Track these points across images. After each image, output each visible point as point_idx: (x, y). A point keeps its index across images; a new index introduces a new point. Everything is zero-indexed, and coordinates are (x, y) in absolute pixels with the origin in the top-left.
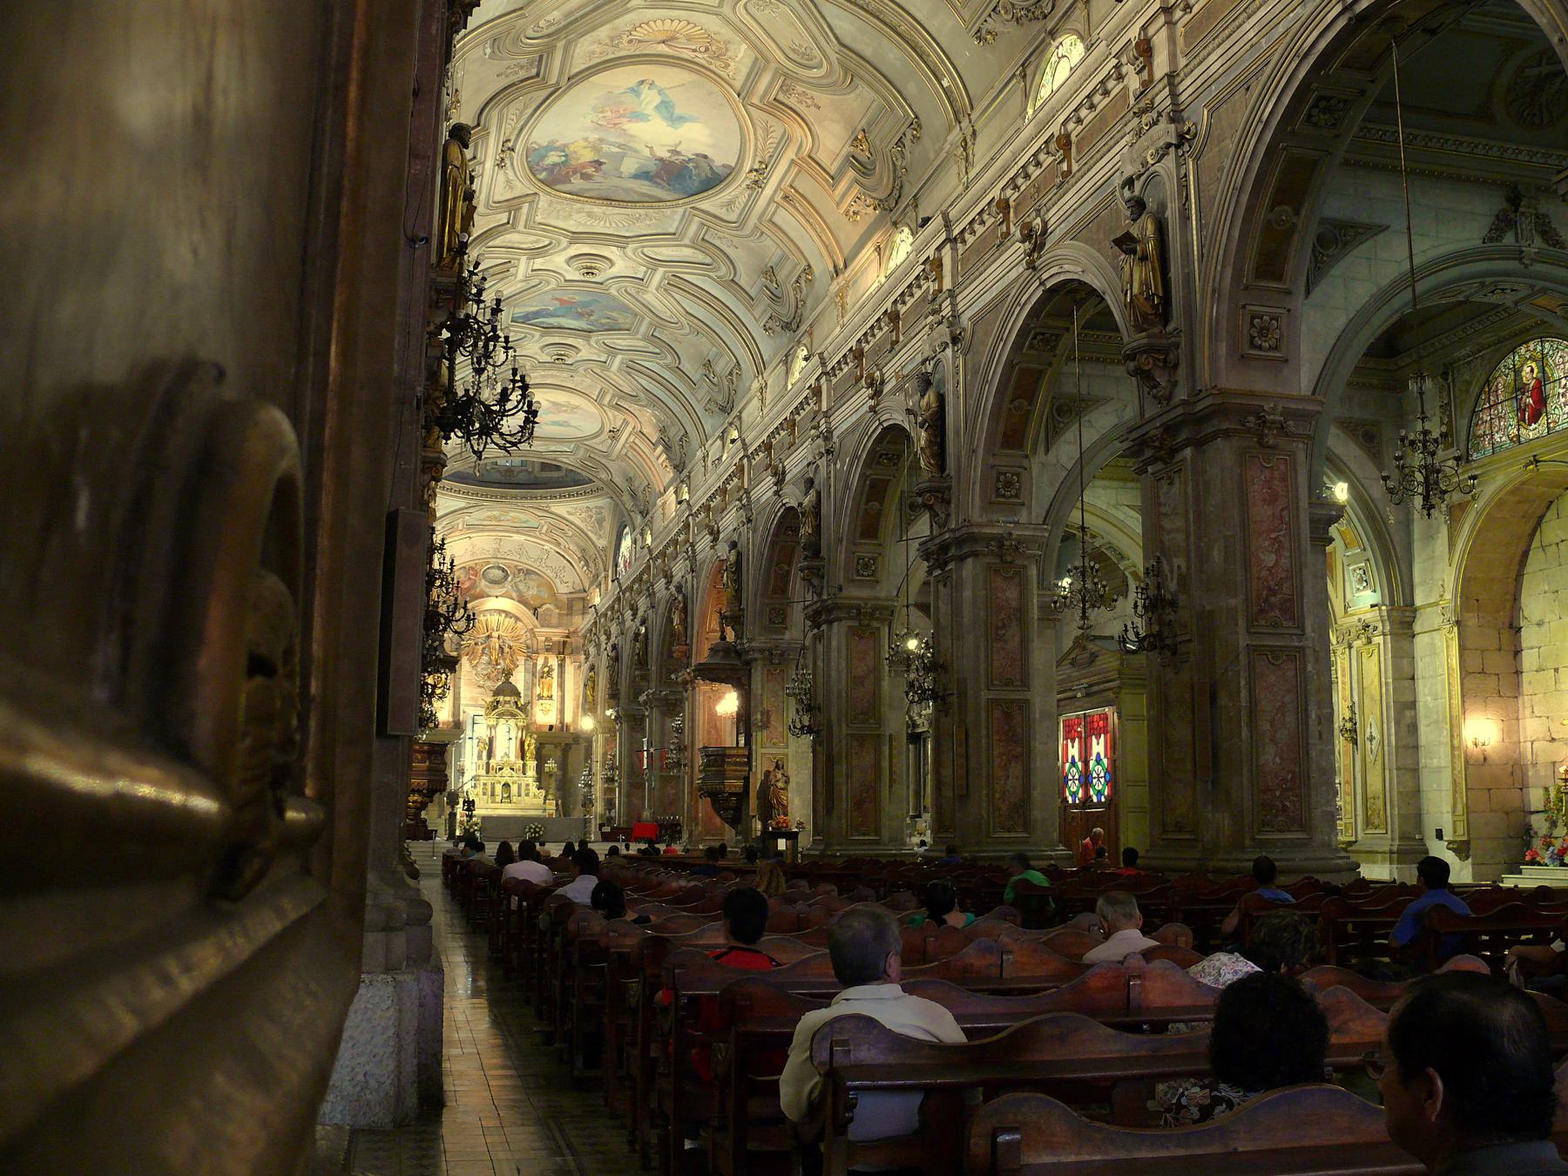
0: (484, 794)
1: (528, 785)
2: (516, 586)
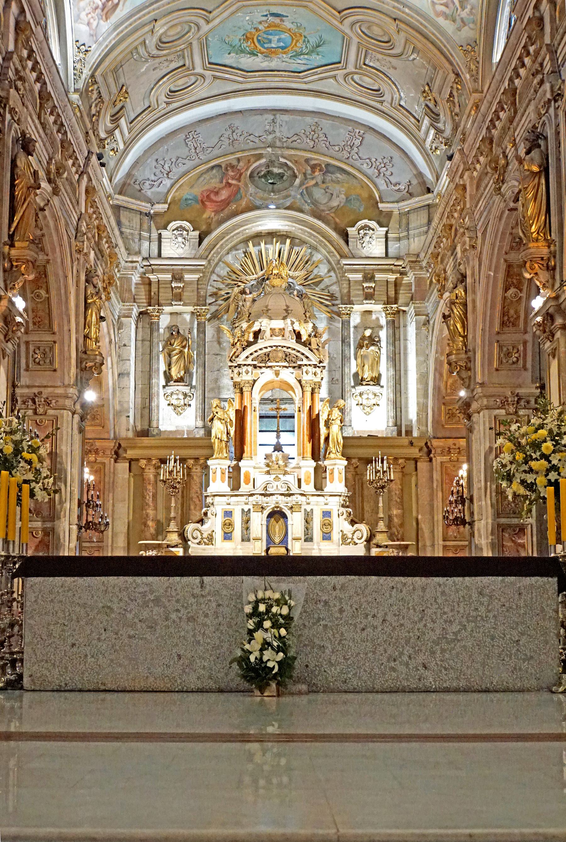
0: (227, 536)
1: (327, 514)
2: (310, 195)
